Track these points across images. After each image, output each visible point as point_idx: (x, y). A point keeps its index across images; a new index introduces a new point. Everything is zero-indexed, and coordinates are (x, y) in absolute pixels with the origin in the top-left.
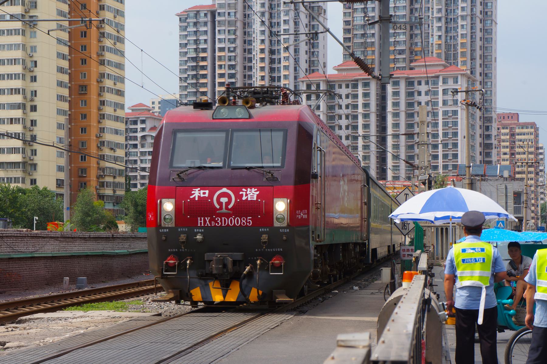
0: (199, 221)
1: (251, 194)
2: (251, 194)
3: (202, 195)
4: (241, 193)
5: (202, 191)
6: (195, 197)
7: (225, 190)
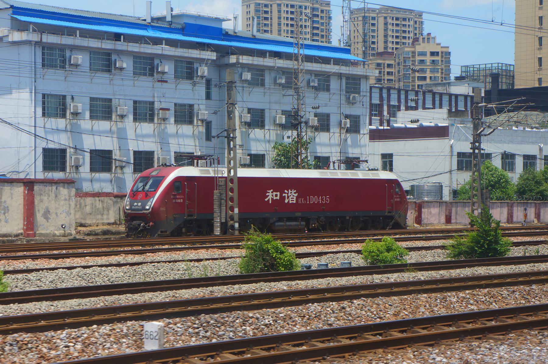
1: (292, 197)
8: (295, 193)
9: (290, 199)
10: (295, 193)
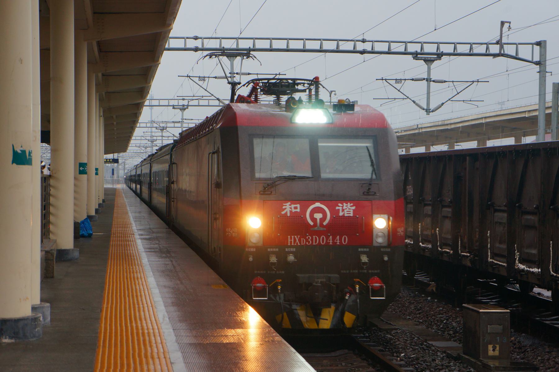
0: (289, 240)
2: (347, 210)
3: (294, 210)
4: (337, 208)
5: (293, 206)
6: (287, 212)
7: (318, 205)
8: (351, 206)
9: (346, 213)
10: (351, 206)
